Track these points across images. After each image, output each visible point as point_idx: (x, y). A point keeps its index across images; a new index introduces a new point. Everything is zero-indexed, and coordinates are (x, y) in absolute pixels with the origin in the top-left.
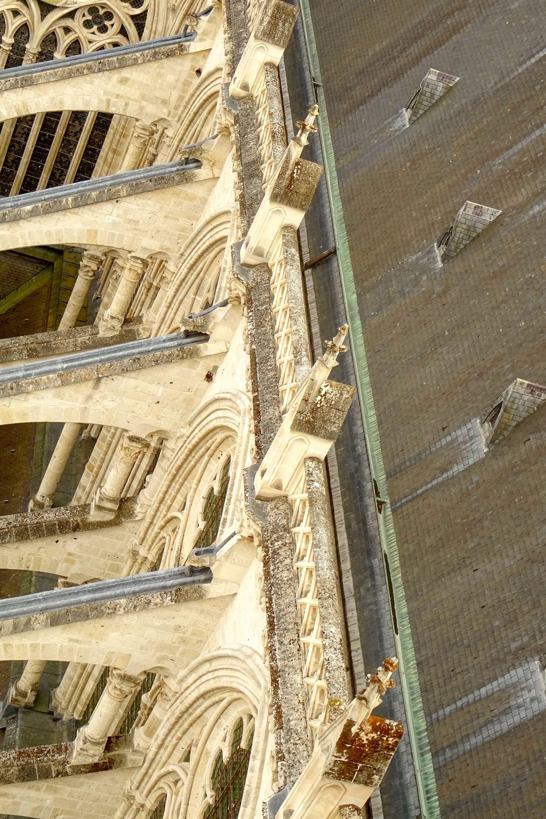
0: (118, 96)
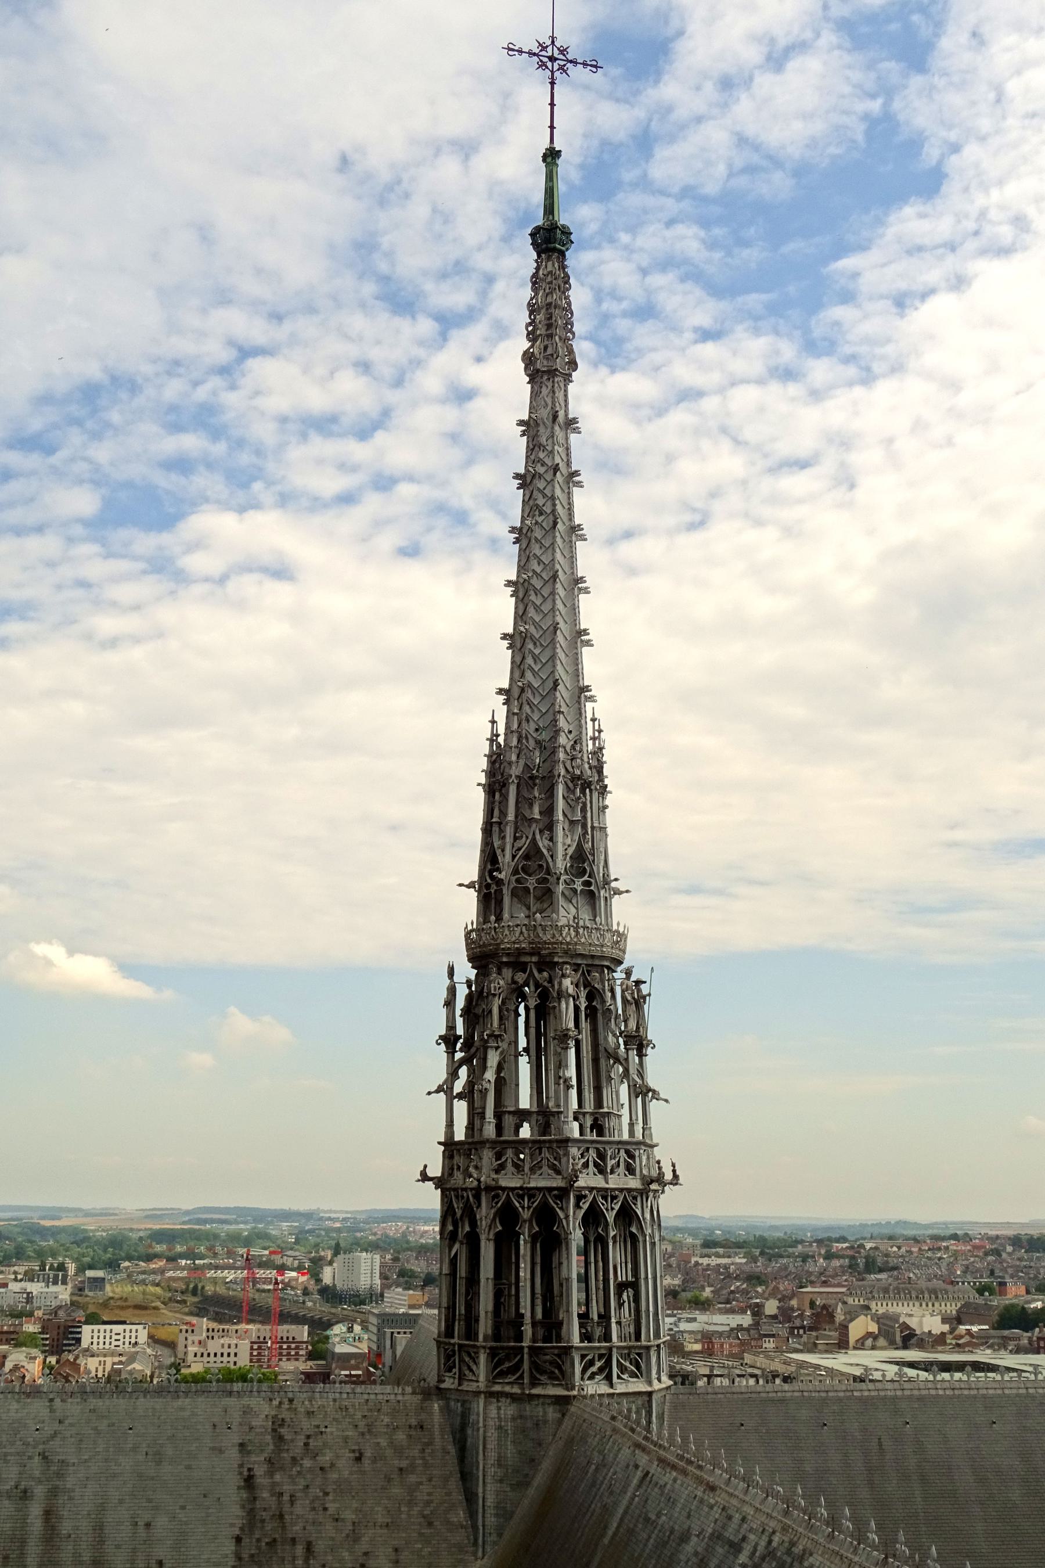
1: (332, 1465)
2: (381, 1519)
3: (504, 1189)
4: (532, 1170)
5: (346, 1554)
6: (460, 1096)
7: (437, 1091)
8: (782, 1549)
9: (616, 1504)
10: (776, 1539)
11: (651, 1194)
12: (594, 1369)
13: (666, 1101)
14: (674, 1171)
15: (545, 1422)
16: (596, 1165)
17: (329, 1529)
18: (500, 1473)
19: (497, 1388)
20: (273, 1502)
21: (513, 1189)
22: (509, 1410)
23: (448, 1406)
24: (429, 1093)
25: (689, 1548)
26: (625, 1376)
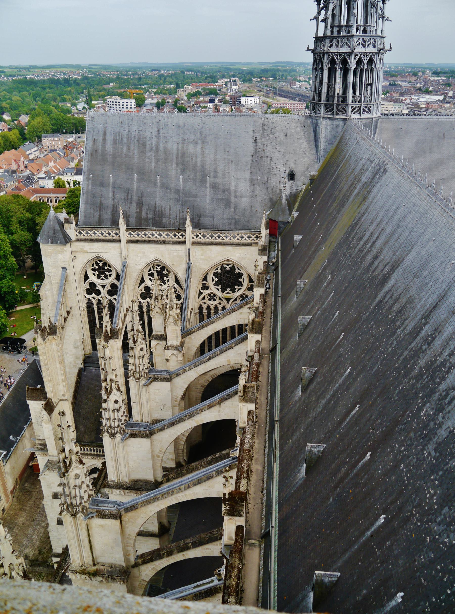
0: (241, 318)
1: (278, 137)
2: (291, 152)
3: (331, 53)
4: (341, 47)
5: (281, 161)
6: (322, 21)
7: (314, 19)
8: (382, 163)
9: (349, 149)
10: (381, 160)
11: (380, 54)
12: (355, 111)
13: (391, 21)
14: (390, 46)
15: (339, 126)
16: (362, 44)
17: (277, 154)
18: (325, 140)
19: (326, 116)
20: (262, 146)
21: (334, 53)
22: (329, 122)
23: (312, 121)
24: (311, 20)
25: (361, 162)
26: (365, 113)
